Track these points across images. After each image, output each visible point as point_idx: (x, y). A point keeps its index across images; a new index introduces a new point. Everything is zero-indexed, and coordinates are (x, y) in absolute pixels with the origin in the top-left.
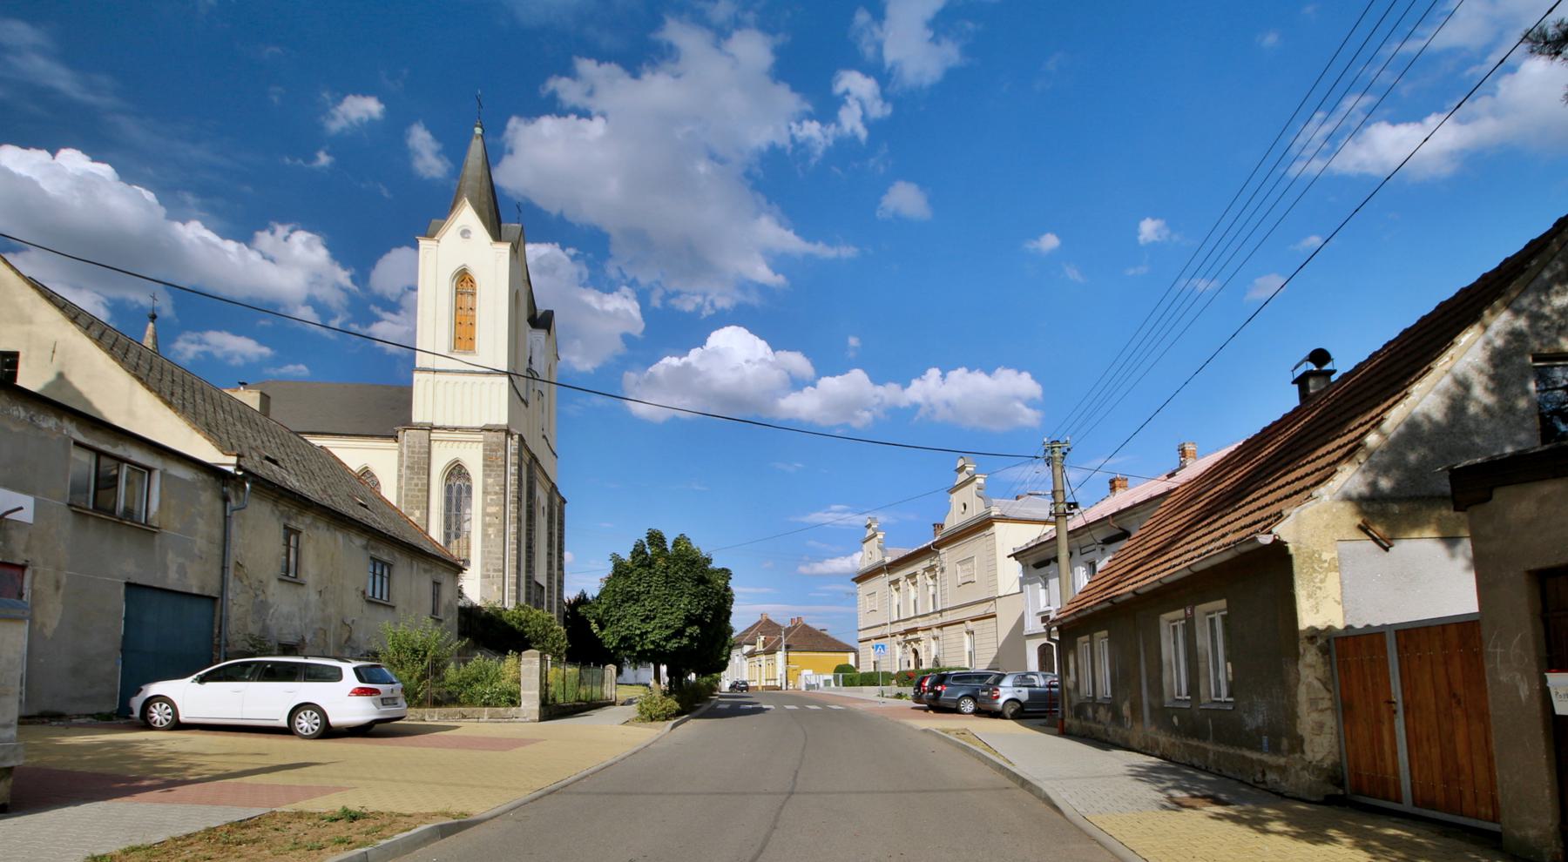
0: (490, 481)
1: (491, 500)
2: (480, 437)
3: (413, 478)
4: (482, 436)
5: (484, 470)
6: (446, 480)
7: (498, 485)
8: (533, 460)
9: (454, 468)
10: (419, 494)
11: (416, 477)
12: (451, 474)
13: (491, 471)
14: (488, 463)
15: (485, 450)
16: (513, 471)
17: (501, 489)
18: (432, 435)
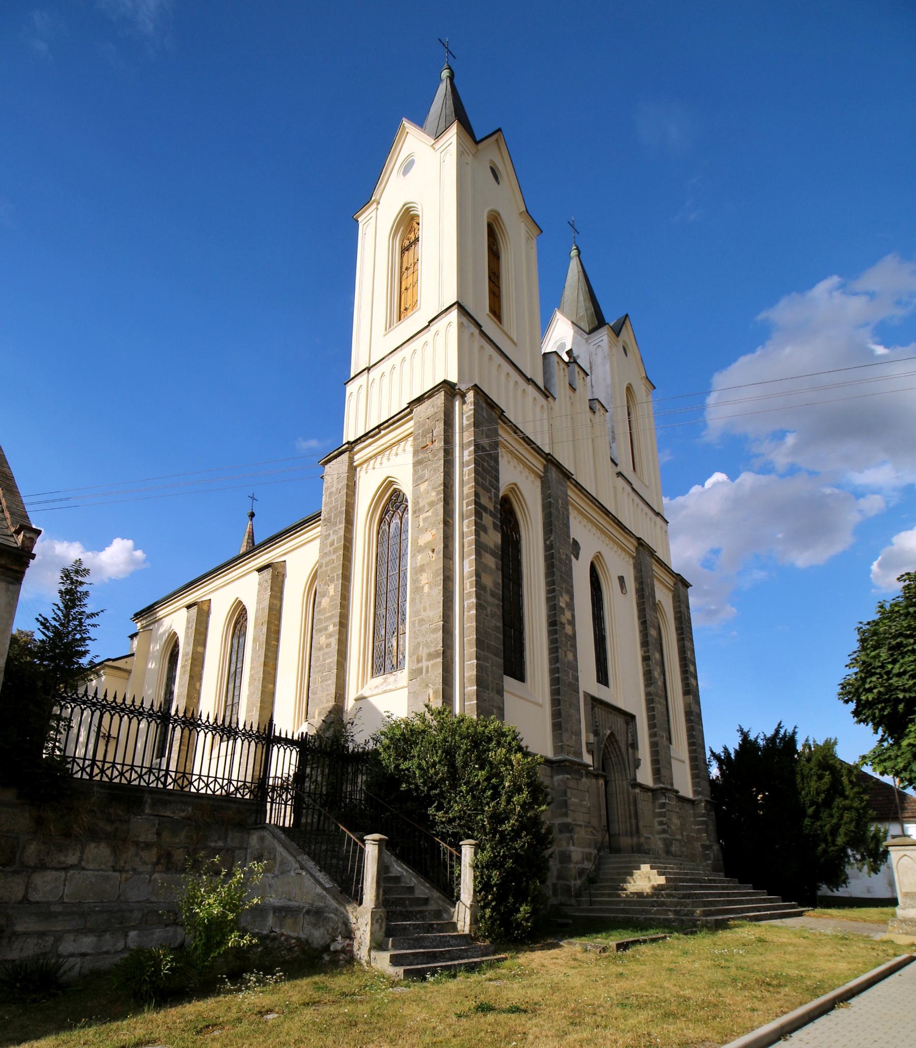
0: (423, 487)
1: (425, 520)
2: (408, 427)
3: (329, 535)
4: (411, 423)
5: (415, 472)
6: (381, 520)
7: (433, 489)
8: (554, 473)
9: (390, 499)
10: (334, 557)
11: (331, 532)
12: (385, 511)
13: (426, 467)
14: (421, 456)
15: (414, 440)
16: (466, 458)
17: (438, 495)
18: (356, 457)
